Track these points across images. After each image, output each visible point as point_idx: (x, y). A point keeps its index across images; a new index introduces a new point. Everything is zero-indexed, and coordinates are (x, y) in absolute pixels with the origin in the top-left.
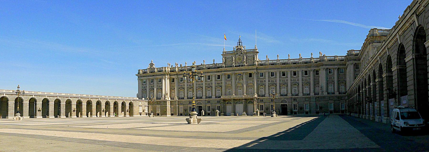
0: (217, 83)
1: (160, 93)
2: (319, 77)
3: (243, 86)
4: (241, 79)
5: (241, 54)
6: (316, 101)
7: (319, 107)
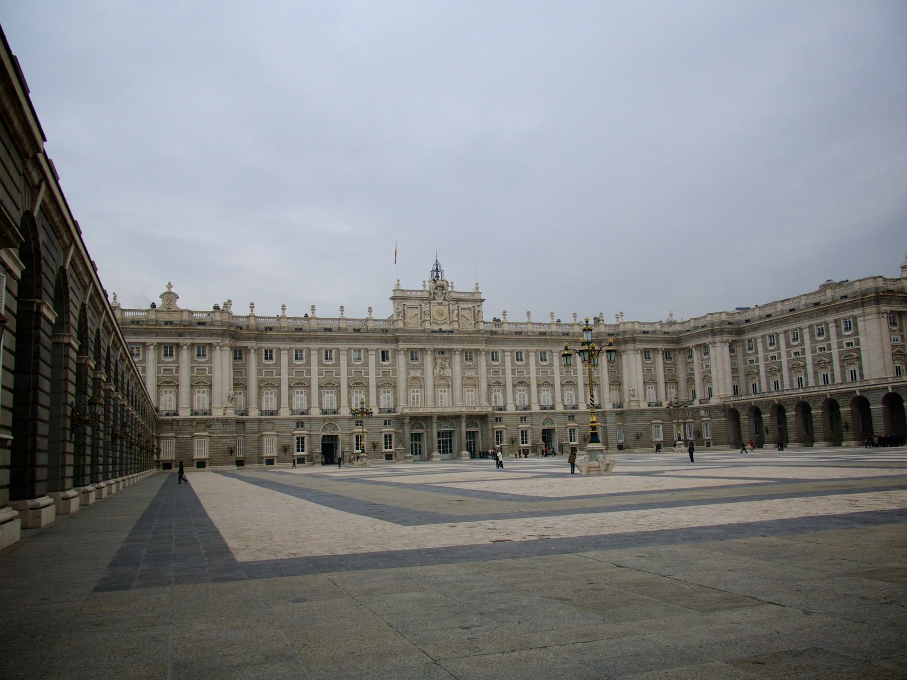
0: (381, 371)
3: (452, 386)
4: (447, 365)
5: (443, 300)
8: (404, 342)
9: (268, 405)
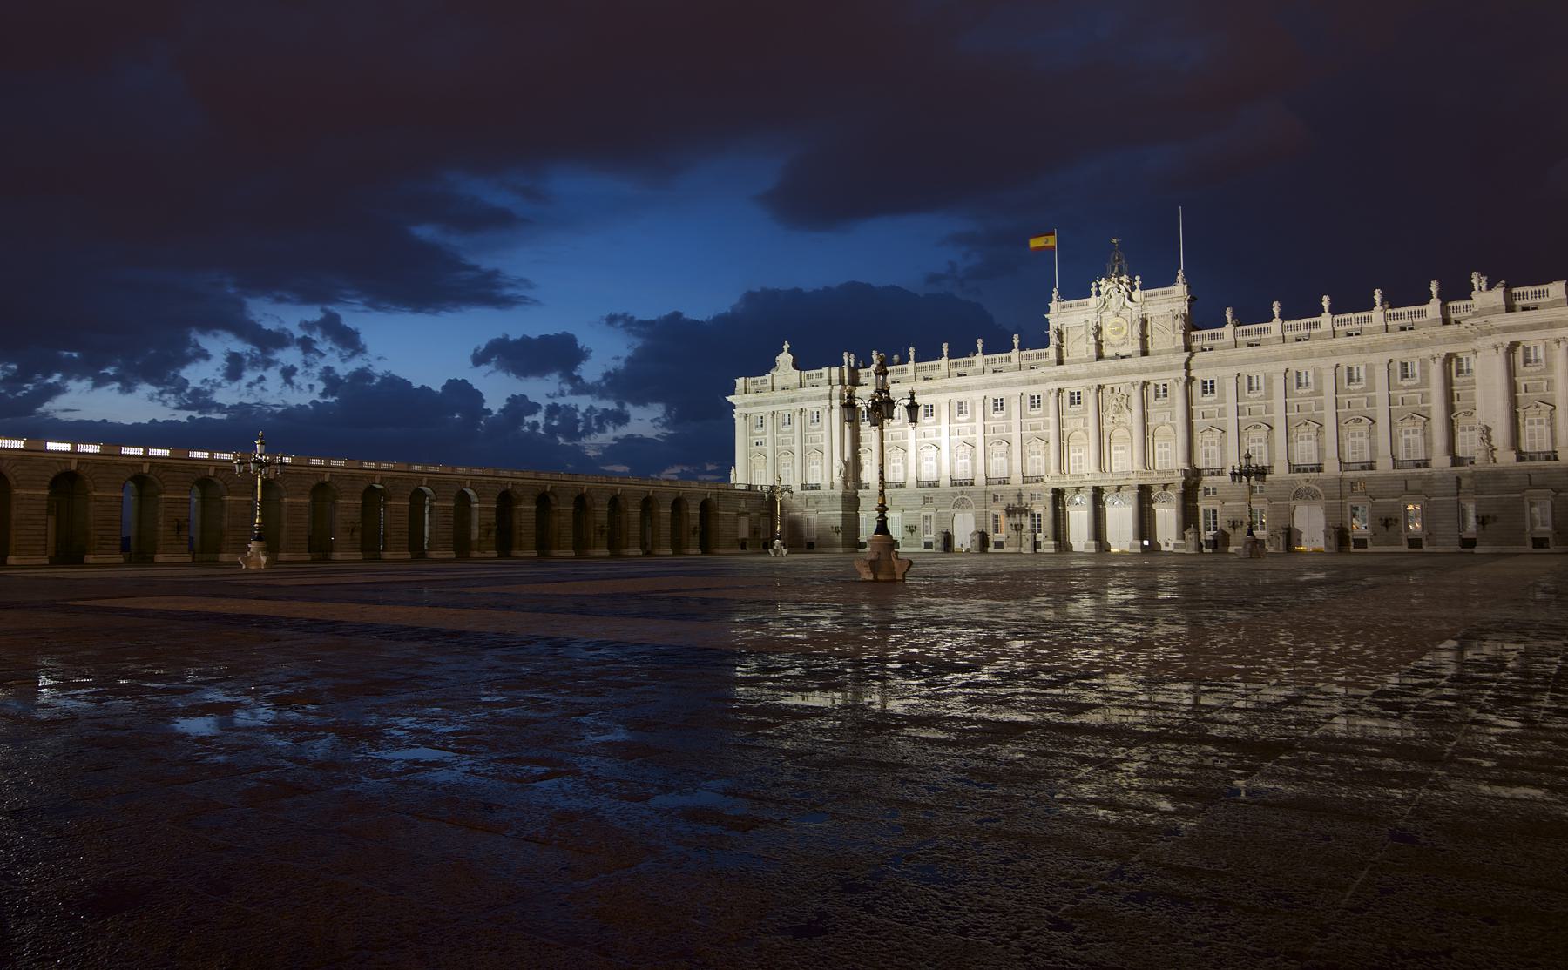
1: (817, 464)
2: (1474, 384)
4: (1125, 409)
5: (1122, 308)
6: (1458, 493)
7: (1477, 517)
8: (1056, 380)
9: (894, 475)
